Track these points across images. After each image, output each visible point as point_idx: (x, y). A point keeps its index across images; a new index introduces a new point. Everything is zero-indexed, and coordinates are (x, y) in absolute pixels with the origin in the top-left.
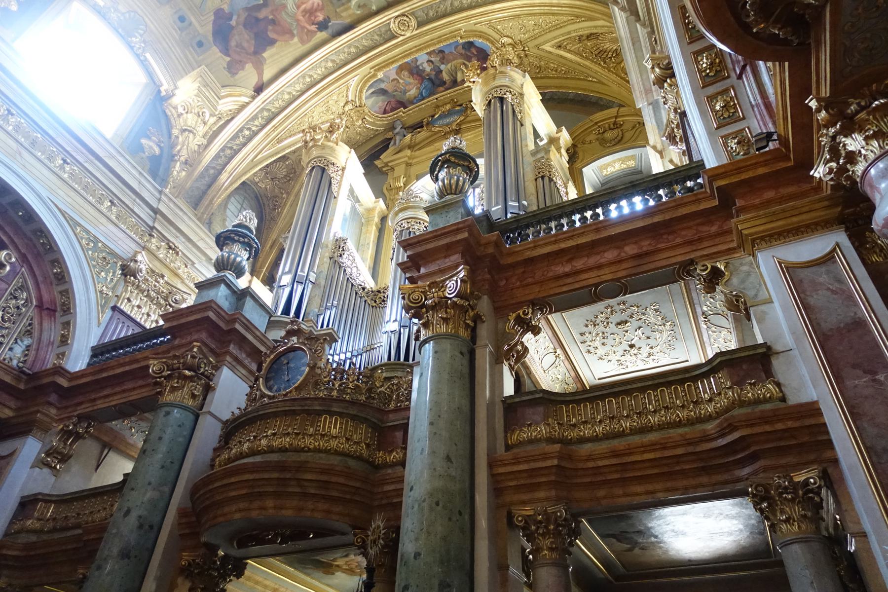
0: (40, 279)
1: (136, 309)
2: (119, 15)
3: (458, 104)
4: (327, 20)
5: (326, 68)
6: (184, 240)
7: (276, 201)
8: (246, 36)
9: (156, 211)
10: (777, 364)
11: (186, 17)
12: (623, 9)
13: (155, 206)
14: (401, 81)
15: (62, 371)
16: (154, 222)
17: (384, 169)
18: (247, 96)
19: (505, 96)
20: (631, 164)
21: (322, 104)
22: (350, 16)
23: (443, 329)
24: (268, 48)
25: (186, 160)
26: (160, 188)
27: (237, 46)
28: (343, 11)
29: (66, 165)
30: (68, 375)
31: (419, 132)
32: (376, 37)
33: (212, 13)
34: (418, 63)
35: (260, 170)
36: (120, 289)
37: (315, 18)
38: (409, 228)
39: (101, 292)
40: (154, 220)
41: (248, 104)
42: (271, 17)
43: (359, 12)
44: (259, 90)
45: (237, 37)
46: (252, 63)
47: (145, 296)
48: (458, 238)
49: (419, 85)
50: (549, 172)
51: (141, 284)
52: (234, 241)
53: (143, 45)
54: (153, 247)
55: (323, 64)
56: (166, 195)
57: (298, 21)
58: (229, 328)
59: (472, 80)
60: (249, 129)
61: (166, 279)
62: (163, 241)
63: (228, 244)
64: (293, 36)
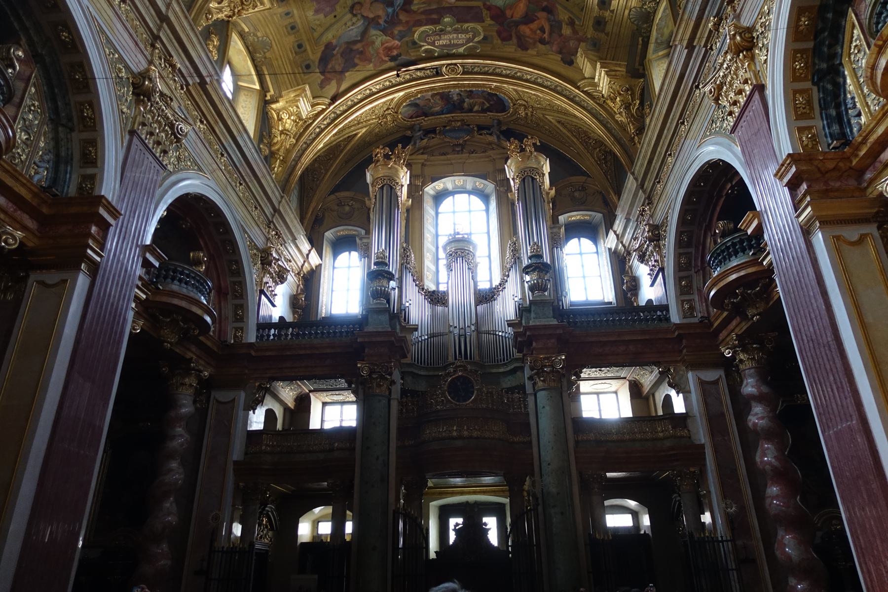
3: (467, 123)
4: (399, 55)
5: (383, 85)
9: (276, 210)
10: (689, 421)
12: (636, 179)
14: (432, 101)
16: (273, 218)
20: (587, 218)
22: (417, 55)
31: (433, 138)
40: (273, 216)
42: (362, 49)
44: (334, 99)
45: (334, 62)
52: (384, 277)
53: (263, 60)
55: (382, 83)
57: (378, 53)
60: (319, 127)
64: (370, 62)
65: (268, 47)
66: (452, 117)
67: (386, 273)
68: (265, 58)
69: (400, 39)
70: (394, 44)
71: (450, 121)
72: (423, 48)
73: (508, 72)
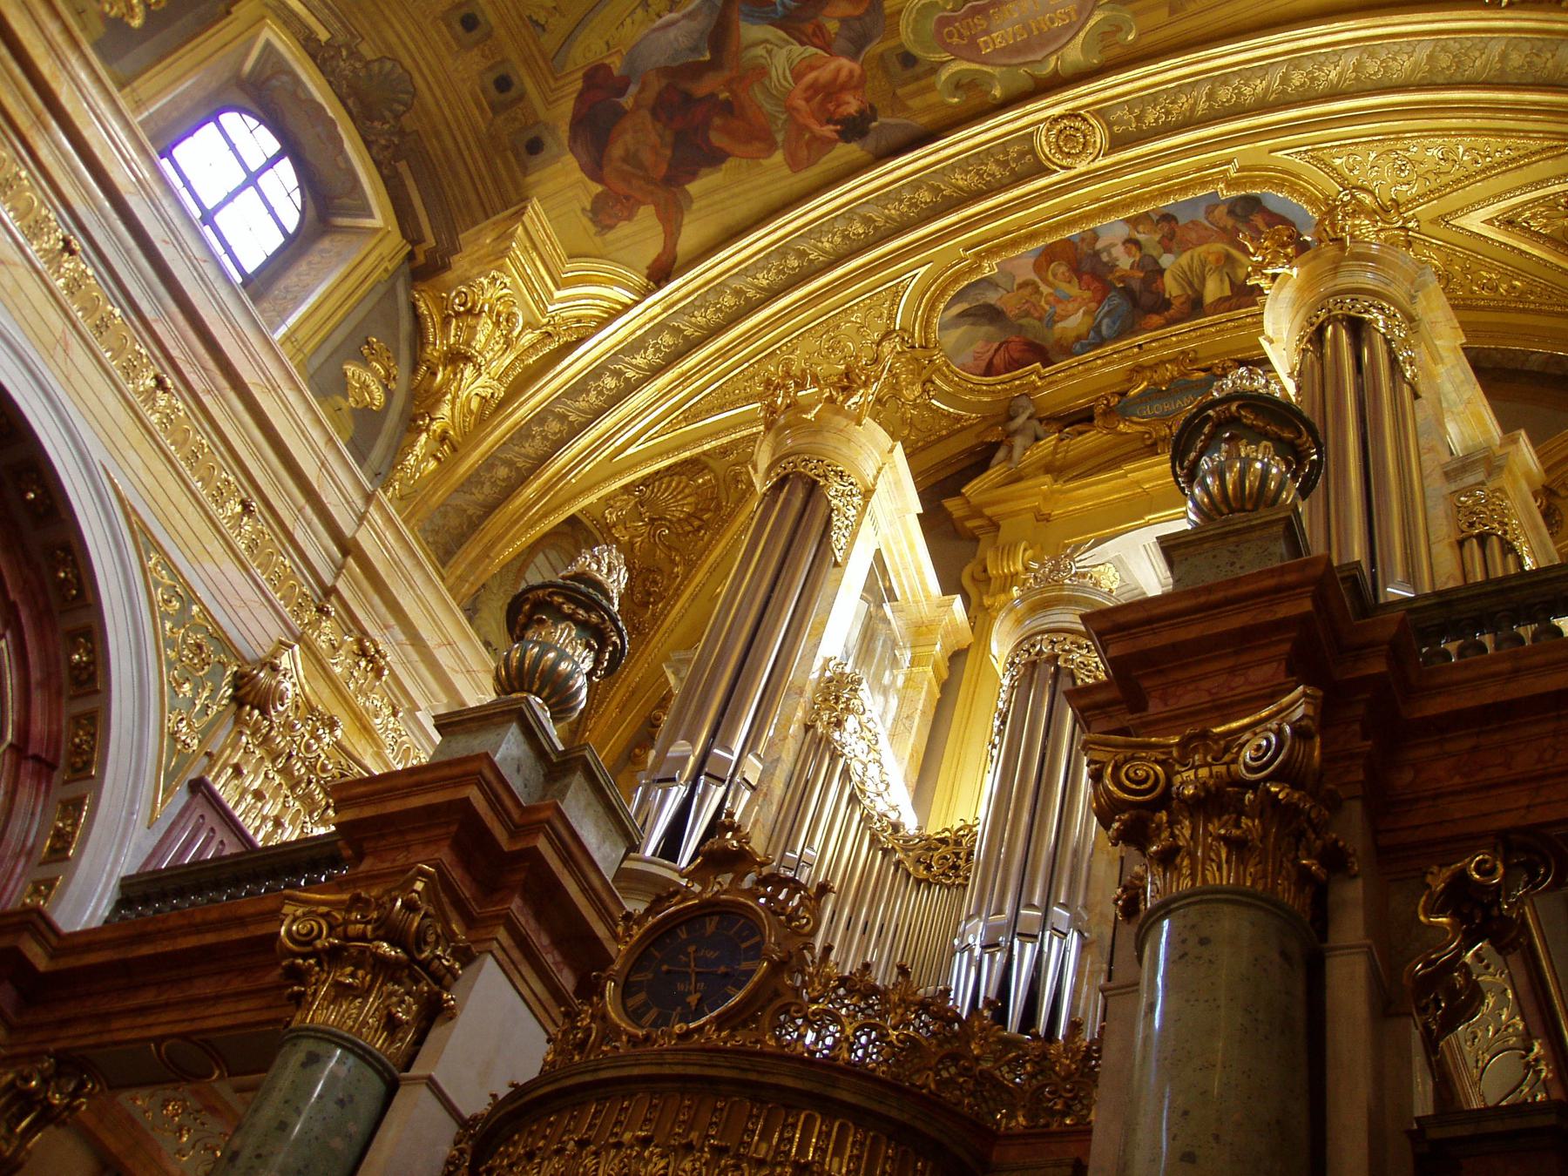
0: (36, 675)
1: (249, 797)
2: (358, 65)
5: (845, 237)
6: (402, 637)
7: (655, 582)
8: (654, 138)
9: (348, 547)
11: (515, 80)
13: (348, 532)
14: (1045, 289)
15: (42, 926)
16: (337, 576)
17: (970, 524)
18: (627, 288)
19: (1366, 316)
21: (822, 329)
22: (929, 108)
23: (1221, 875)
24: (704, 171)
25: (445, 432)
26: (369, 487)
27: (625, 160)
28: (913, 95)
29: (159, 393)
30: (53, 940)
31: (1080, 433)
32: (992, 167)
33: (580, 74)
34: (1099, 246)
35: (626, 489)
36: (223, 735)
37: (838, 106)
38: (1056, 657)
39: (174, 736)
40: (339, 570)
41: (627, 308)
42: (724, 95)
43: (956, 100)
44: (660, 274)
45: (628, 137)
46: (657, 206)
47: (279, 771)
48: (1280, 615)
49: (1093, 305)
50: (1502, 523)
51: (273, 733)
54: (322, 644)
55: (839, 226)
56: (381, 507)
57: (791, 110)
58: (519, 846)
59: (1269, 271)
60: (618, 374)
61: (338, 733)
62: (349, 632)
63: (541, 621)
64: (772, 147)
65: (404, 97)
66: (1140, 346)
67: (569, 599)
68: (402, 133)
69: (857, 46)
70: (838, 71)
71: (1138, 369)
72: (944, 75)
73: (1260, 86)
